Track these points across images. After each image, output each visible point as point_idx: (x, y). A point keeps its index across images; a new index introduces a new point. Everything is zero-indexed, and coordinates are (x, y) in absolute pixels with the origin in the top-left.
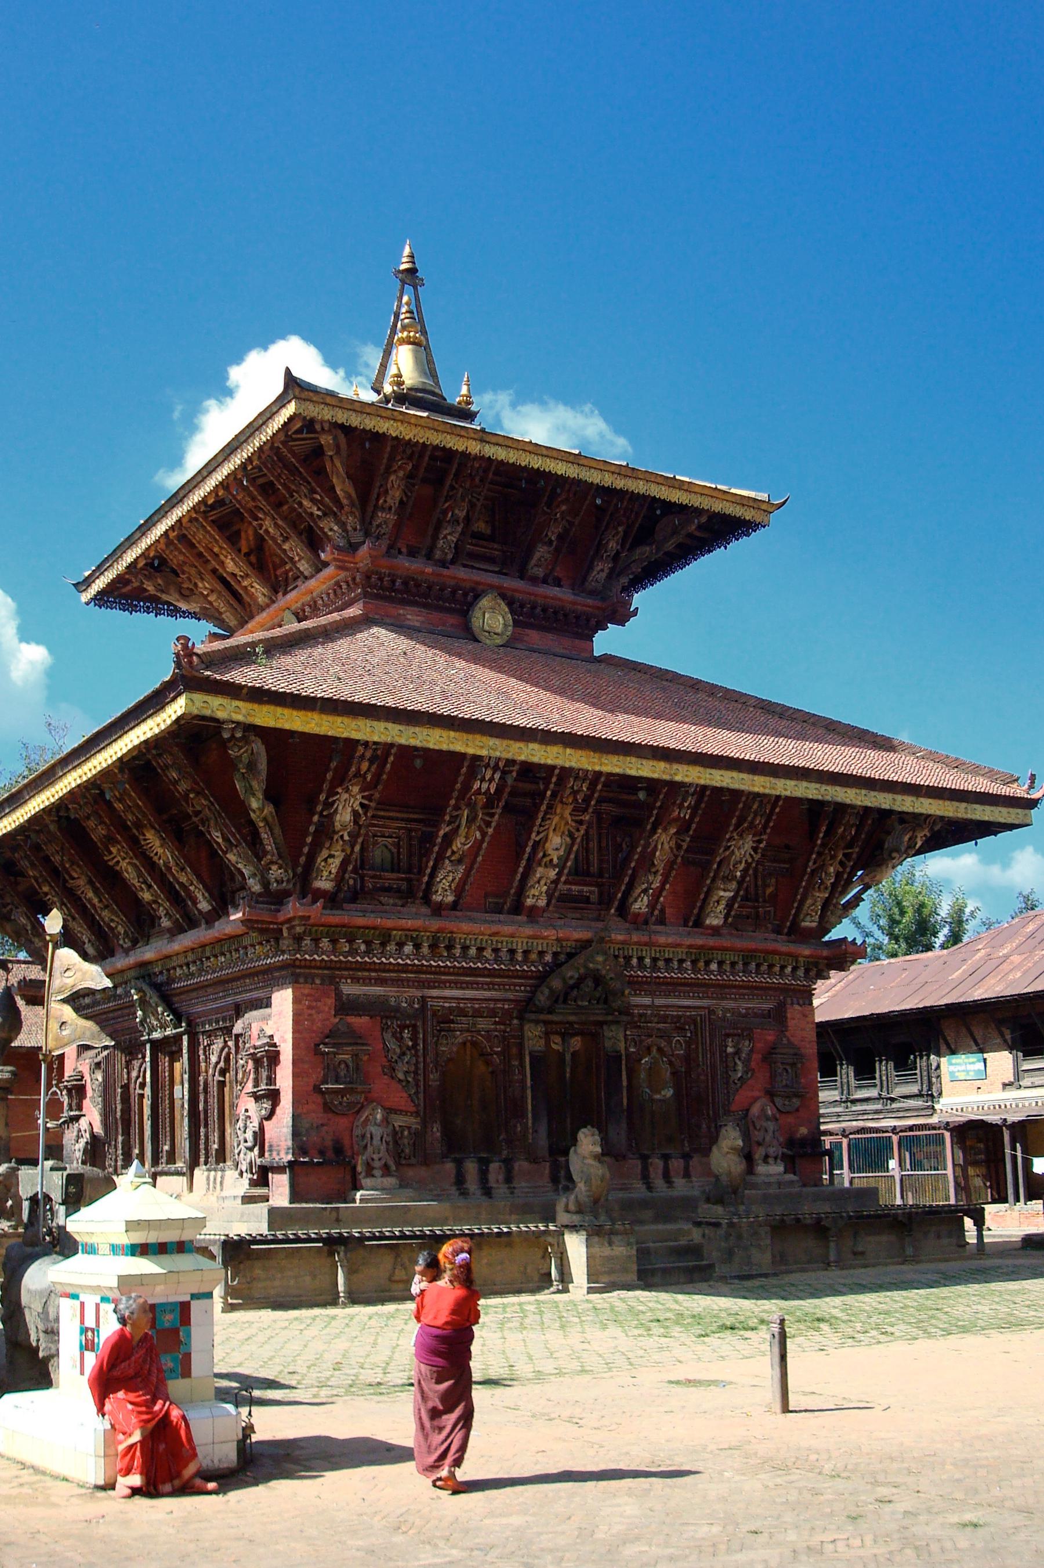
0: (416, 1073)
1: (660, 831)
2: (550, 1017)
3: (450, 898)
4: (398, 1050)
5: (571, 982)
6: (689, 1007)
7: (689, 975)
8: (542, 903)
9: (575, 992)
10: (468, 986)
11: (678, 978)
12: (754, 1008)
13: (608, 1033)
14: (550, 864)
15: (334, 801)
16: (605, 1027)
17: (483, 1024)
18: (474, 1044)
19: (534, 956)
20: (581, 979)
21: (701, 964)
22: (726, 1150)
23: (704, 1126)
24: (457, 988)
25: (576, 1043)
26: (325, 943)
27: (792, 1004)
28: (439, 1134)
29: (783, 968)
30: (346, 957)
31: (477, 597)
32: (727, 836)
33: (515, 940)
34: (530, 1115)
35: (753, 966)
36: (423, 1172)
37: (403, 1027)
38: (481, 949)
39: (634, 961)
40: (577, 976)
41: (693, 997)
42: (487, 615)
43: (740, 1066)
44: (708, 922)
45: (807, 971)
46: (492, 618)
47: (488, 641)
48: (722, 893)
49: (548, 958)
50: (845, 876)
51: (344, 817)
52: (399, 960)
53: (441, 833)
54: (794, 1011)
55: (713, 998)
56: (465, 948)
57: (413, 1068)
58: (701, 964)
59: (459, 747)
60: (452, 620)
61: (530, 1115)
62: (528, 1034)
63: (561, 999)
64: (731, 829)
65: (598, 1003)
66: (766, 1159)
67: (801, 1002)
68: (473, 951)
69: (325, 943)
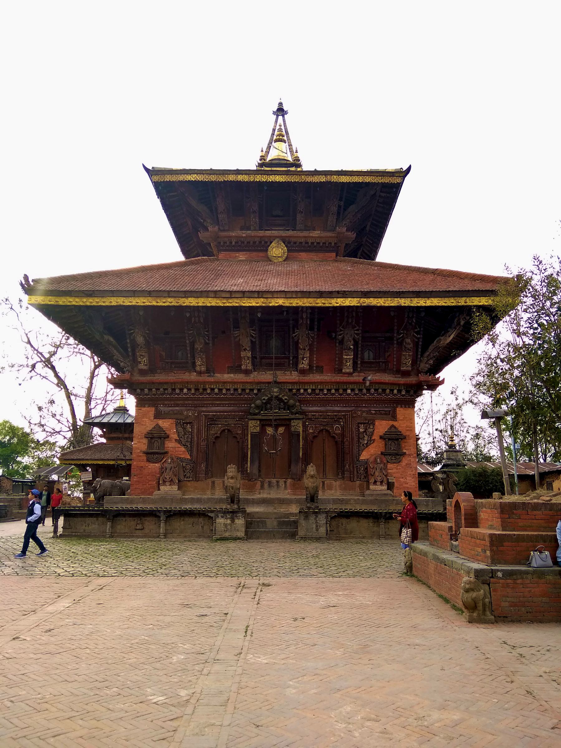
0: (191, 442)
1: (296, 330)
2: (260, 417)
3: (203, 369)
4: (183, 433)
5: (264, 401)
6: (339, 411)
8: (250, 367)
9: (269, 406)
10: (218, 405)
12: (379, 411)
13: (293, 424)
14: (245, 350)
15: (133, 333)
16: (292, 421)
17: (231, 422)
18: (229, 430)
19: (247, 391)
20: (270, 399)
21: (341, 391)
22: (308, 476)
23: (347, 466)
25: (281, 430)
26: (146, 391)
29: (392, 390)
31: (271, 243)
32: (338, 330)
34: (249, 460)
37: (187, 423)
38: (220, 390)
39: (302, 391)
40: (266, 398)
42: (274, 250)
43: (366, 438)
45: (407, 392)
46: (277, 250)
47: (275, 261)
48: (345, 357)
49: (255, 392)
50: (420, 343)
51: (140, 340)
53: (187, 342)
54: (400, 411)
56: (213, 390)
57: (190, 440)
58: (341, 391)
59: (154, 303)
60: (261, 254)
61: (249, 460)
62: (250, 425)
64: (338, 326)
66: (375, 483)
68: (216, 391)
69: (146, 391)
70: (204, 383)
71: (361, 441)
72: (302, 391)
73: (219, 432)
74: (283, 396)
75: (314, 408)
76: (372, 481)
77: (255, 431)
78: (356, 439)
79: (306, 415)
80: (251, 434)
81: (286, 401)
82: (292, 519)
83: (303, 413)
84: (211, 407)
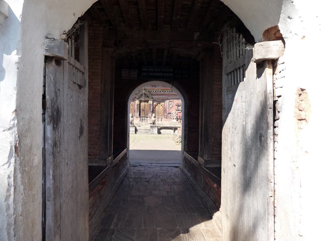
2: (140, 99)
7: (163, 93)
39: (152, 92)
72: (152, 92)
75: (156, 97)
76: (172, 118)
83: (153, 98)
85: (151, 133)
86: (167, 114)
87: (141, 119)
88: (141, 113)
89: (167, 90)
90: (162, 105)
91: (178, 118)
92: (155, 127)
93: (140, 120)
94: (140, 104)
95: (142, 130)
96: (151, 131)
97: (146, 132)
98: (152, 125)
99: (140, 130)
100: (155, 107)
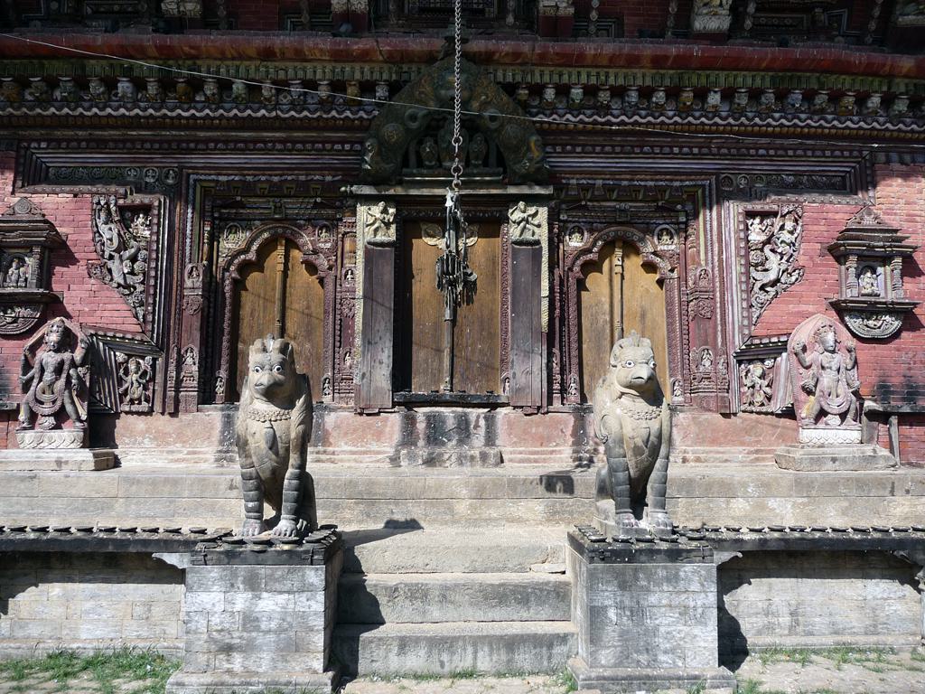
5: (414, 125)
7: (671, 117)
10: (248, 146)
11: (649, 123)
21: (688, 96)
24: (235, 150)
27: (888, 161)
28: (195, 368)
29: (862, 99)
30: (31, 109)
33: (309, 65)
35: (797, 96)
36: (160, 421)
39: (550, 94)
41: (682, 155)
43: (774, 263)
44: (698, 24)
52: (122, 111)
55: (723, 157)
58: (688, 96)
63: (413, 158)
65: (486, 164)
67: (907, 158)
70: (194, 57)
71: (754, 274)
72: (550, 94)
73: (255, 247)
74: (485, 105)
75: (589, 162)
77: (380, 238)
78: (736, 269)
79: (559, 188)
80: (367, 253)
81: (493, 125)
82: (541, 574)
84: (223, 151)
85: (606, 656)
86: (722, 363)
87: (421, 426)
88: (419, 356)
89: (723, 78)
90: (650, 267)
91: (869, 404)
92: (675, 555)
93: (409, 438)
94: (402, 251)
95: (446, 594)
96: (610, 634)
97: (512, 644)
98: (608, 519)
99: (418, 594)
100: (581, 285)
